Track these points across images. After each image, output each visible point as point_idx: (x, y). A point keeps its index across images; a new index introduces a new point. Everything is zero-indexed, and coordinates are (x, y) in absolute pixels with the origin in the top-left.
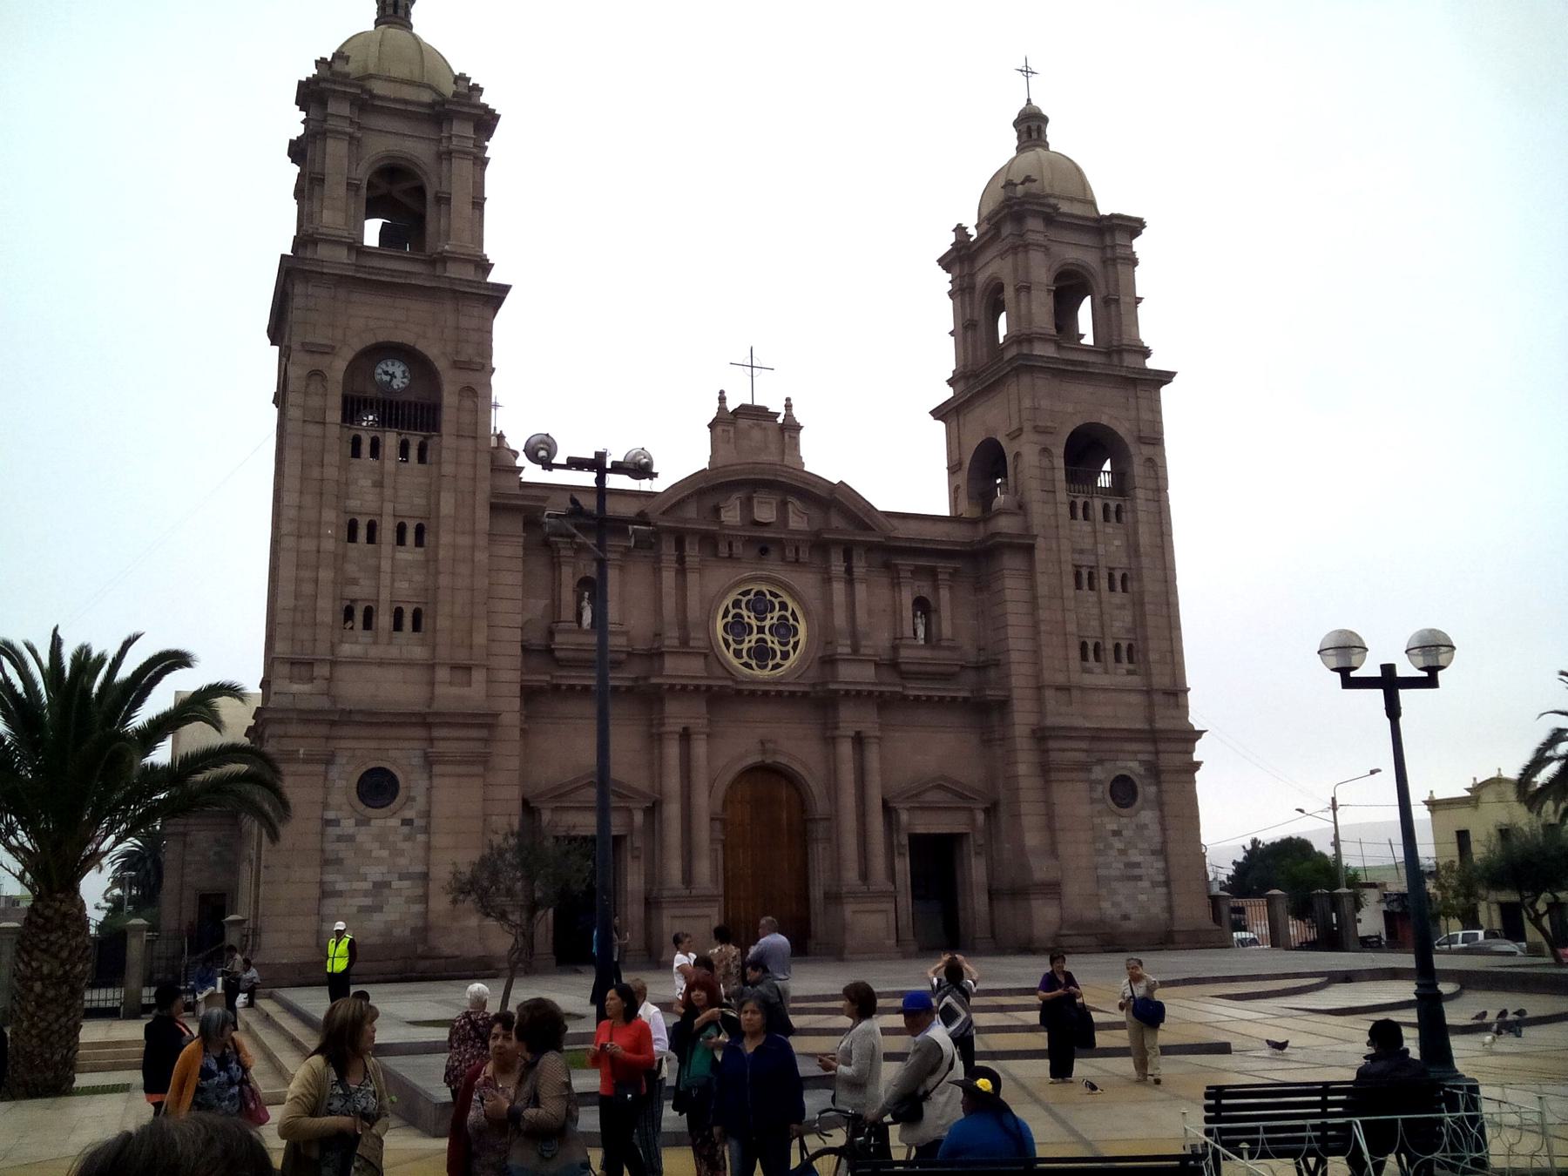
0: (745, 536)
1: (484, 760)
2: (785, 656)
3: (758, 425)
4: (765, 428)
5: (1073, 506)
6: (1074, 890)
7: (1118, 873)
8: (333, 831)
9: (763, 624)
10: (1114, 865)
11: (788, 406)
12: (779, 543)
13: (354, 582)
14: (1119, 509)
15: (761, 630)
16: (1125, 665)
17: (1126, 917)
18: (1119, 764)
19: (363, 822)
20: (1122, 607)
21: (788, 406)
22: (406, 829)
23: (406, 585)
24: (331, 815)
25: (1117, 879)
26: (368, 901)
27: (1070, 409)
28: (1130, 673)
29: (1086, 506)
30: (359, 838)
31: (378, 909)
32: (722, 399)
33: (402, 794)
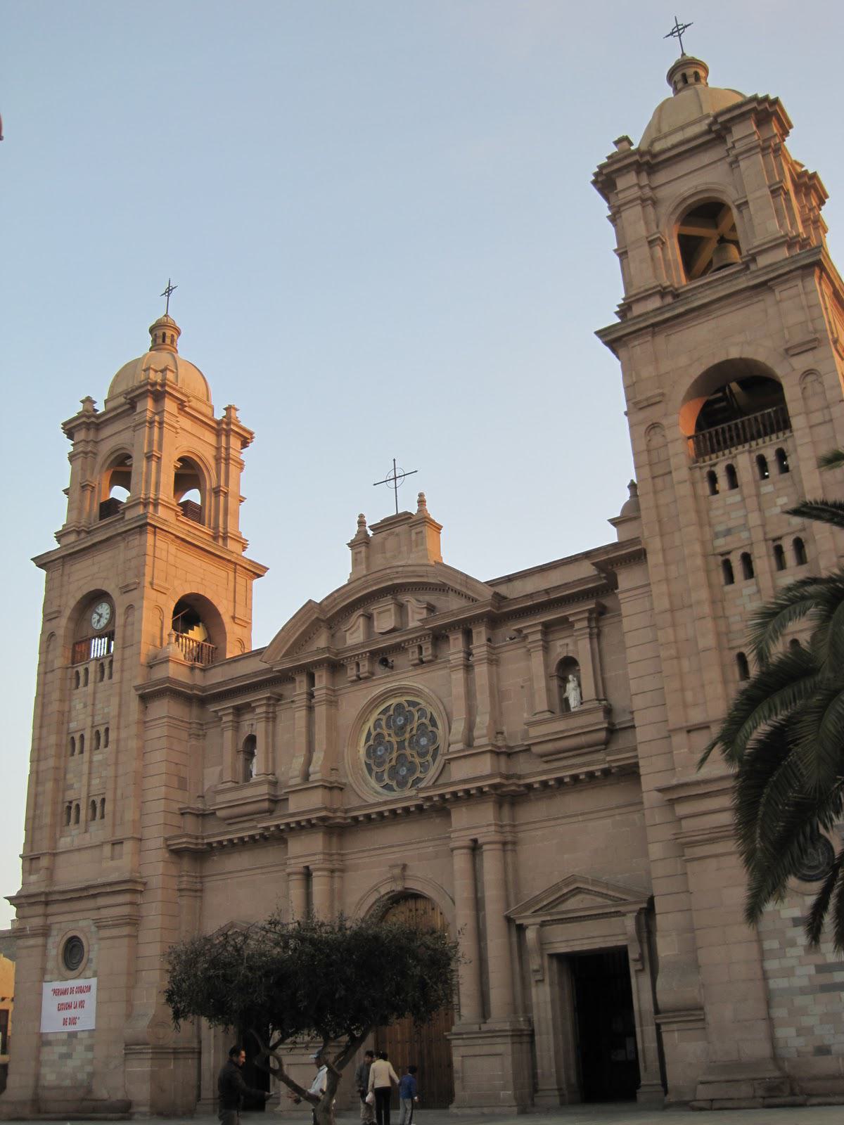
0: (365, 653)
1: (134, 921)
2: (425, 767)
3: (392, 534)
4: (397, 535)
5: (713, 478)
6: (720, 1012)
7: (805, 982)
10: (799, 971)
11: (421, 502)
12: (398, 648)
14: (781, 455)
17: (823, 1051)
21: (421, 502)
25: (803, 991)
26: (64, 1050)
27: (683, 361)
29: (731, 471)
31: (67, 1056)
32: (361, 523)
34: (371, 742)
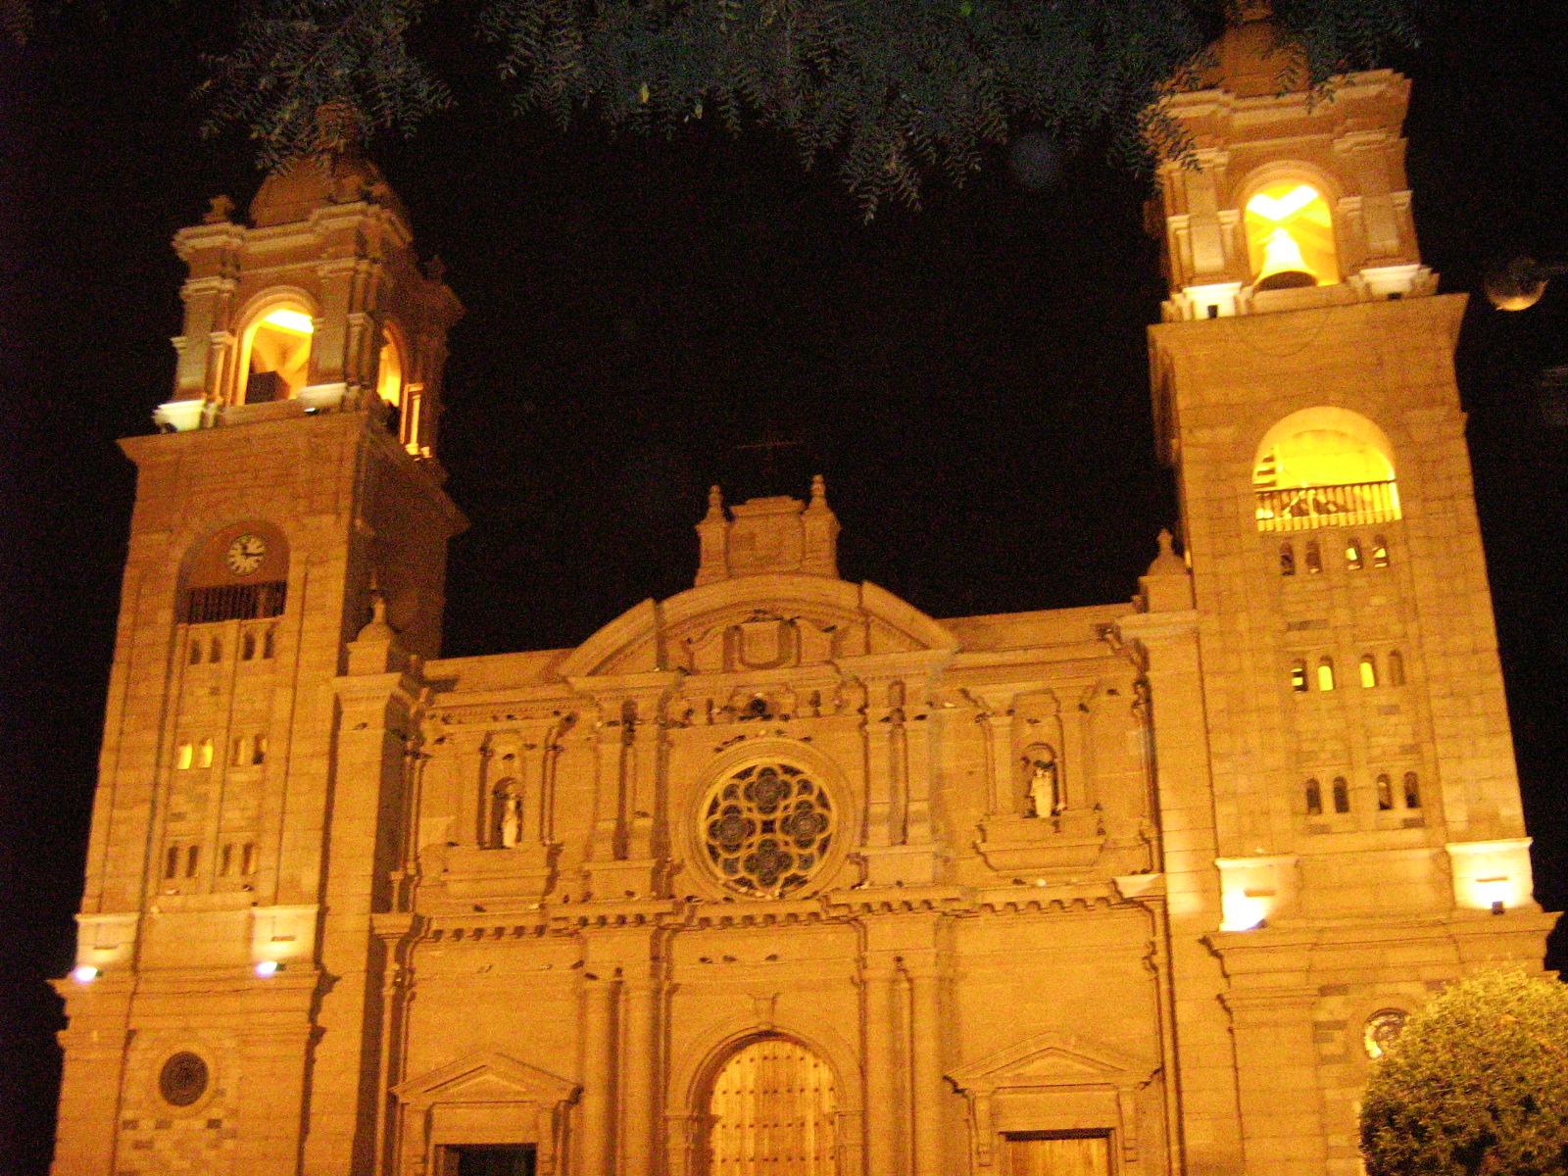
8: (128, 1136)
9: (771, 817)
13: (179, 817)
15: (768, 827)
16: (1401, 811)
18: (1381, 988)
19: (162, 1125)
20: (1392, 710)
22: (212, 1133)
23: (237, 814)
24: (128, 1114)
28: (1409, 824)
30: (158, 1145)
33: (211, 1086)
34: (717, 816)
